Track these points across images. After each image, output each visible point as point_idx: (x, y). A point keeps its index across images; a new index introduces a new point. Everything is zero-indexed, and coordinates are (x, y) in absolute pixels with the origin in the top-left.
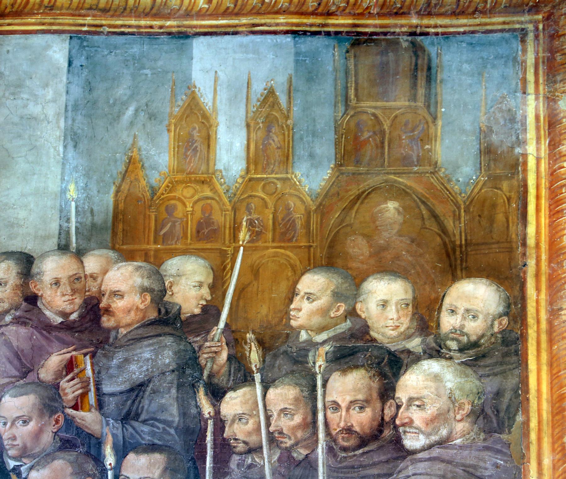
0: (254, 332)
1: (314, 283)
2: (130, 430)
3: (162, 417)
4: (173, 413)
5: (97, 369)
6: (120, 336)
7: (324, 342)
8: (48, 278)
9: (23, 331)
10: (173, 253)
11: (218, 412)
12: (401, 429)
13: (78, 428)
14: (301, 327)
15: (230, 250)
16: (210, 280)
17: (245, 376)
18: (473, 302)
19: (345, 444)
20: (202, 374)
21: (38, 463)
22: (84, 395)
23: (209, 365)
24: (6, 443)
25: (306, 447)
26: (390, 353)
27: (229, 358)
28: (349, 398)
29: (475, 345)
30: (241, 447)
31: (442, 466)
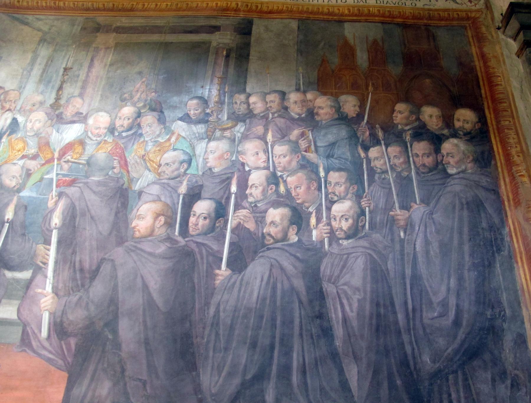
0: (379, 125)
1: (400, 107)
2: (331, 162)
3: (343, 157)
4: (348, 155)
5: (314, 136)
6: (323, 124)
7: (408, 130)
8: (292, 101)
9: (282, 120)
10: (343, 94)
11: (367, 156)
12: (446, 166)
13: (307, 160)
14: (398, 124)
15: (366, 93)
16: (359, 104)
17: (377, 142)
18: (465, 117)
19: (423, 171)
20: (359, 139)
21: (291, 174)
22: (309, 147)
23: (361, 137)
24: (276, 165)
25: (406, 171)
26: (436, 135)
27: (370, 134)
28: (422, 152)
29: (469, 133)
30: (379, 171)
31: (465, 181)
